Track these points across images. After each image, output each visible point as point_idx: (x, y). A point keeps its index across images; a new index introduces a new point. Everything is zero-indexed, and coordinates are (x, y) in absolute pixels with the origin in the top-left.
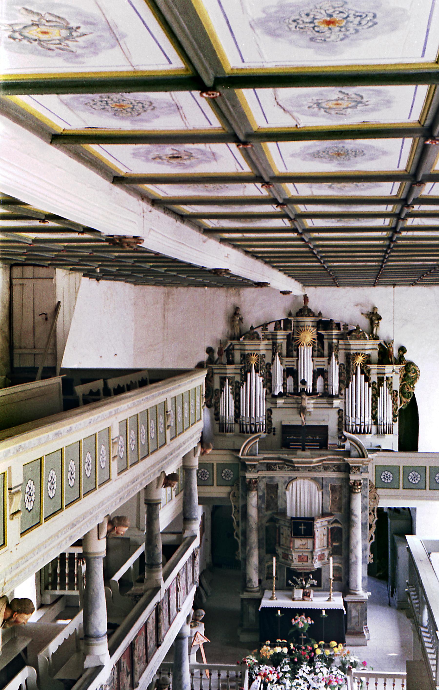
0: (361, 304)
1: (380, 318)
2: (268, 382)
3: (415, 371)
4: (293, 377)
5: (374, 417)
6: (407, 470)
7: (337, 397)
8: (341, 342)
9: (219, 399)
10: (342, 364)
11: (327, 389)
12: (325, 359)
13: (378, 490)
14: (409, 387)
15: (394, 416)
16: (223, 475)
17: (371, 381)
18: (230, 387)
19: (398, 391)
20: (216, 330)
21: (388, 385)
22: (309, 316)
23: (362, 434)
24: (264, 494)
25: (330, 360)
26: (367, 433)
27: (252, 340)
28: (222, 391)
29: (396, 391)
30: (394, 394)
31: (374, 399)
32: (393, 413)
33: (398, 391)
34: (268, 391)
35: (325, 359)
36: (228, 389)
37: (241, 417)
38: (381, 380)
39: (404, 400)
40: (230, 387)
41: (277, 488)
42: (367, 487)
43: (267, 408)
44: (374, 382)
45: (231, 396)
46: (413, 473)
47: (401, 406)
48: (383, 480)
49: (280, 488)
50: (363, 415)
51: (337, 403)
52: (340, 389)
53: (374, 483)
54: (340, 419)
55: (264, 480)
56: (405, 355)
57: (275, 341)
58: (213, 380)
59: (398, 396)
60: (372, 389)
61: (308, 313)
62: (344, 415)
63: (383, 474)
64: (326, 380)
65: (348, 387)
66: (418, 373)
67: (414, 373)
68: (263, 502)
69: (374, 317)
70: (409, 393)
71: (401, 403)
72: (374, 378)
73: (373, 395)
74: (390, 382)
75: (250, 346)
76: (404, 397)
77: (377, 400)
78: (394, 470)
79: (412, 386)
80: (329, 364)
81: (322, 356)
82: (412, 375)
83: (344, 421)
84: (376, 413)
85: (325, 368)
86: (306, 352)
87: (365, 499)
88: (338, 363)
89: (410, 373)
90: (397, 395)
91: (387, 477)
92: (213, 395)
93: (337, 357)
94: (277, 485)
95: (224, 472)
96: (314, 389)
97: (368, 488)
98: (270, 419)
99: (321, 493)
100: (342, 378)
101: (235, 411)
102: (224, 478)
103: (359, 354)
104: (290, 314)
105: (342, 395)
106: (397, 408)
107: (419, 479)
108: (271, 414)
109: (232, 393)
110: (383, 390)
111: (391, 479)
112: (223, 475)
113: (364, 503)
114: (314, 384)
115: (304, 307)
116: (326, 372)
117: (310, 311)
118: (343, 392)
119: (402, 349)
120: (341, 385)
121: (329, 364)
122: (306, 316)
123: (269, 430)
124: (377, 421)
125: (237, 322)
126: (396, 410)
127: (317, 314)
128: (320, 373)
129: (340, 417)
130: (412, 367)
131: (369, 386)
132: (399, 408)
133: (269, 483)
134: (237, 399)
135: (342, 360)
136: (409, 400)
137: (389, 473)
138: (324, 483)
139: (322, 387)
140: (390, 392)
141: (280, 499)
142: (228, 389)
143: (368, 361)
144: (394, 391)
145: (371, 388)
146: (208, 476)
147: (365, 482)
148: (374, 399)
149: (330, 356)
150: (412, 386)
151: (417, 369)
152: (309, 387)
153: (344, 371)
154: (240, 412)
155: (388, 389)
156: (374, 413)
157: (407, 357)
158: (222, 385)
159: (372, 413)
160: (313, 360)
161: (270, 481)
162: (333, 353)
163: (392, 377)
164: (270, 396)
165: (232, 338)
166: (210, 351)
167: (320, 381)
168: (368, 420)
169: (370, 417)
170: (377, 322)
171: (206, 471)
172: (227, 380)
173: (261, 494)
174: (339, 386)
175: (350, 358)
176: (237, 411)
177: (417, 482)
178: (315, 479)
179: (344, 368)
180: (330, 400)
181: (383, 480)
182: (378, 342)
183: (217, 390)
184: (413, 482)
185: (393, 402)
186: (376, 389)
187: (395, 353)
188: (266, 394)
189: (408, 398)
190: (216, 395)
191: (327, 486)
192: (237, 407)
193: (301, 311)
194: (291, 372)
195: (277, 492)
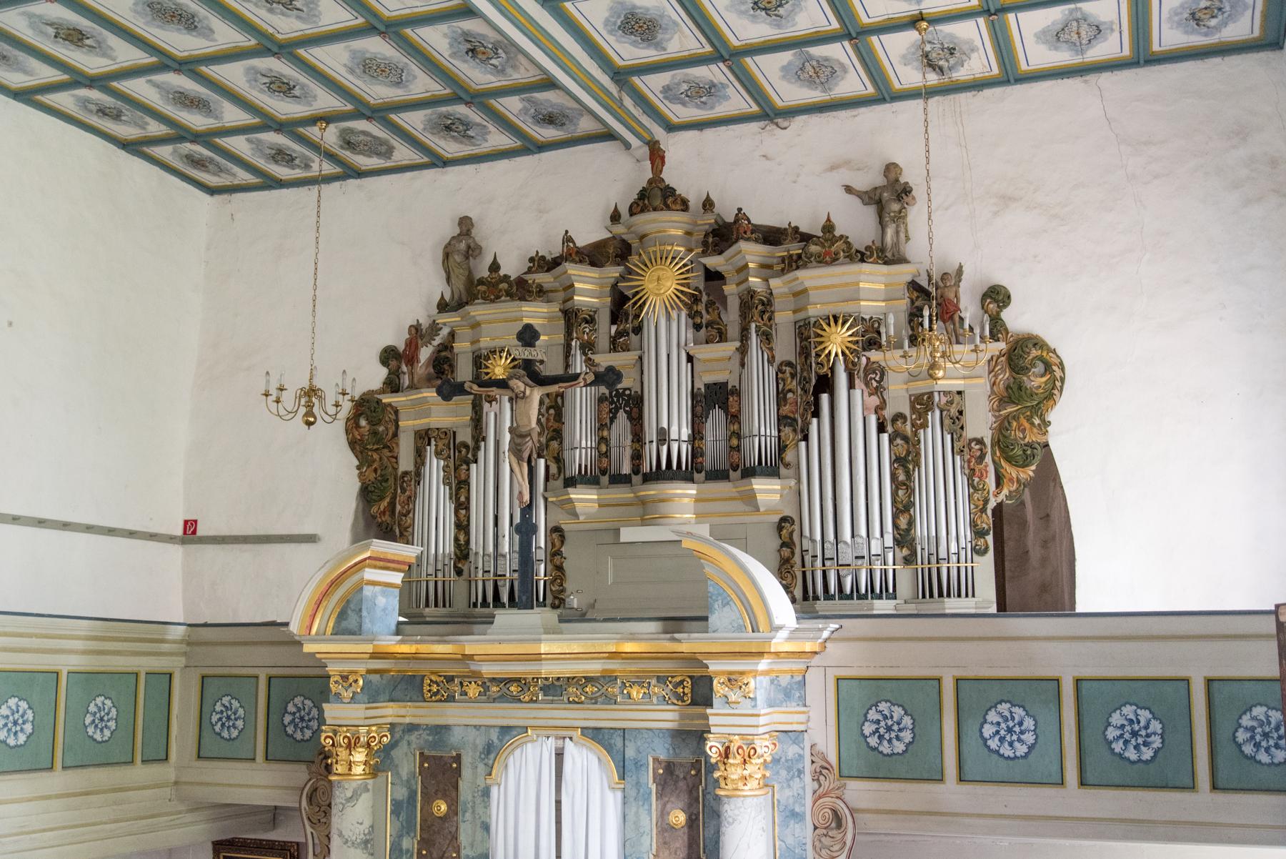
0: (847, 163)
1: (903, 193)
2: (553, 439)
3: (1048, 367)
4: (630, 418)
5: (904, 538)
6: (976, 694)
7: (772, 471)
8: (775, 283)
9: (411, 499)
10: (789, 364)
11: (738, 448)
12: (730, 347)
13: (853, 785)
14: (1027, 425)
15: (979, 533)
16: (287, 719)
17: (888, 413)
18: (442, 463)
19: (988, 441)
20: (406, 292)
21: (947, 422)
22: (668, 208)
23: (860, 597)
24: (412, 795)
25: (743, 350)
26: (880, 597)
27: (492, 301)
28: (418, 475)
29: (980, 441)
30: (970, 452)
31: (902, 477)
32: (973, 524)
33: (988, 441)
34: (554, 469)
35: (730, 347)
36: (435, 468)
37: (472, 558)
38: (922, 403)
39: (1010, 470)
40: (442, 463)
41: (458, 772)
42: (800, 772)
43: (551, 525)
44: (899, 417)
45: (444, 491)
46: (1004, 708)
47: (1001, 497)
48: (873, 741)
49: (466, 772)
50: (863, 532)
51: (767, 490)
52: (782, 448)
53: (833, 758)
54: (786, 552)
55: (413, 737)
56: (1006, 315)
57: (569, 305)
58: (397, 444)
59: (988, 459)
60: (891, 441)
61: (665, 198)
62: (796, 537)
63: (873, 715)
64: (734, 418)
65: (806, 438)
66: (1058, 373)
67: (1042, 376)
68: (408, 828)
69: (889, 197)
70: (1030, 445)
71: (999, 483)
72: (898, 401)
73: (899, 461)
74: (954, 411)
75: (496, 324)
76: (1009, 460)
77: (909, 475)
78: (915, 693)
79: (1037, 421)
80: (743, 365)
81: (722, 337)
82: (1035, 381)
83: (797, 559)
84: (911, 523)
85: (733, 382)
86: (666, 331)
87: (796, 827)
88: (771, 361)
89: (1028, 375)
90: (981, 458)
91: (889, 729)
92: (395, 490)
93: (766, 337)
94: (458, 759)
95: (291, 708)
96: (696, 453)
97: (808, 778)
98: (557, 560)
99: (619, 794)
100: (786, 410)
101: (456, 539)
102: (290, 730)
103: (836, 319)
104: (615, 217)
105: (787, 465)
106: (986, 501)
107: (1029, 738)
108: (563, 543)
109: (446, 482)
110: (933, 440)
111: (907, 736)
112: (287, 719)
113: (790, 841)
114: (696, 435)
115: (650, 182)
116: (737, 392)
117: (669, 192)
118: (789, 456)
119: (996, 297)
120: (787, 430)
121: (743, 365)
122: (655, 210)
123: (555, 598)
124: (914, 553)
125: (458, 258)
126: (983, 510)
127: (695, 200)
128: (715, 399)
129: (783, 545)
130: (1034, 353)
131: (881, 428)
132: (992, 504)
133: (426, 752)
134: (463, 499)
135: (785, 348)
136: (1030, 471)
137: (898, 712)
138: (630, 753)
139: (722, 445)
140: (958, 445)
141: (468, 815)
142: (435, 468)
143: (871, 337)
144: (971, 441)
145: (885, 437)
146: (240, 724)
147: (792, 750)
148: (902, 477)
149: (744, 337)
150: (1037, 421)
151: (1054, 360)
152: (680, 448)
153: (793, 384)
154: (468, 542)
155: (948, 437)
156: (903, 522)
157: (1017, 319)
158: (420, 454)
159: (895, 526)
160: (690, 359)
161: (434, 745)
162: (753, 325)
163: (959, 393)
164: (560, 483)
165: (443, 307)
166: (388, 356)
167: (715, 425)
168: (882, 542)
169: (889, 541)
170: (895, 207)
171: (235, 704)
172: (433, 443)
173: (402, 793)
174: (779, 437)
175: (807, 334)
176: (462, 537)
177: (1021, 750)
178: (596, 735)
179: (793, 376)
180: (743, 486)
181: (873, 741)
182: (903, 273)
183: (406, 473)
184: (1006, 751)
185: (970, 485)
186: (905, 439)
187: (969, 309)
188: (547, 478)
189: (1025, 465)
190: (404, 491)
191: (639, 765)
192: (462, 526)
193: (643, 194)
194: (624, 403)
195: (456, 788)
